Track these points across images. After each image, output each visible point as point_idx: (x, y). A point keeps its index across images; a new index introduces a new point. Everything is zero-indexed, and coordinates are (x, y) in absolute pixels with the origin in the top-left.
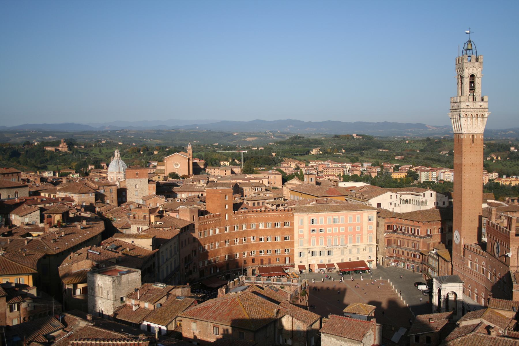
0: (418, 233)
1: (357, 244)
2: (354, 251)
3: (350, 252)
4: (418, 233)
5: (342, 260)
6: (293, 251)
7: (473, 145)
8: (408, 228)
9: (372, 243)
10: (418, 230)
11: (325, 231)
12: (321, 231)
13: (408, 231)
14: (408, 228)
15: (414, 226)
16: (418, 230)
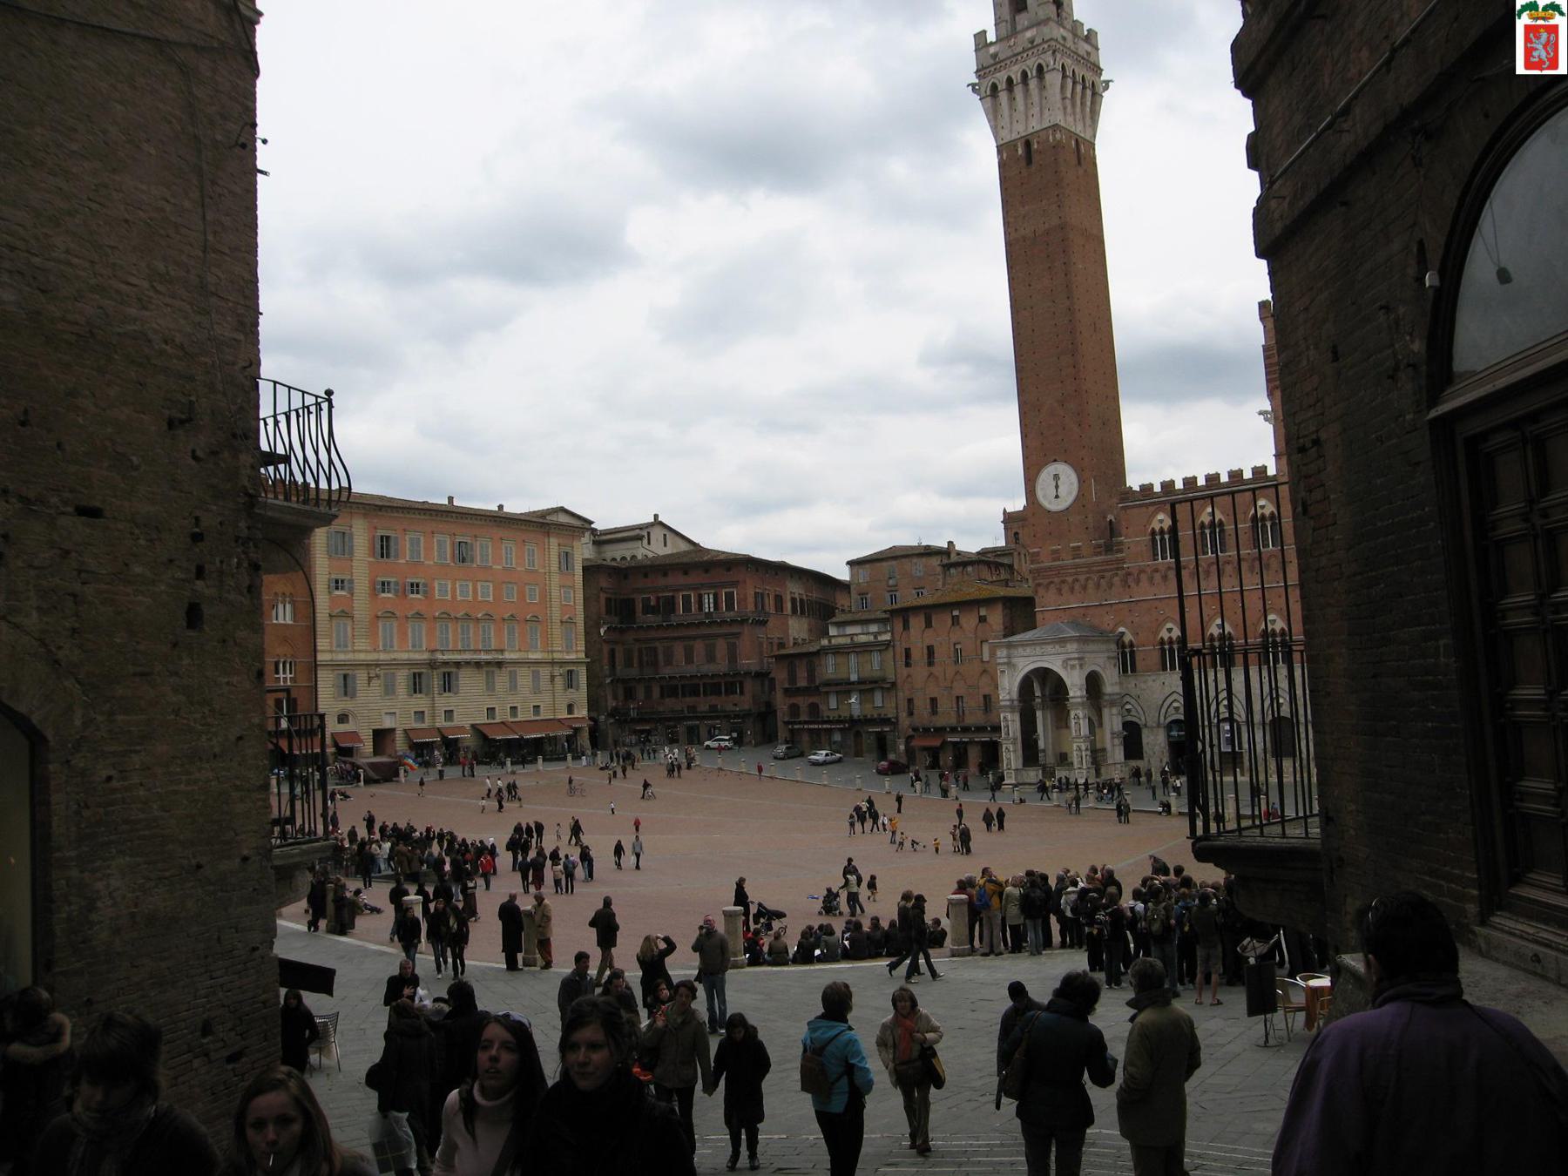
0: (730, 606)
1: (533, 656)
2: (524, 678)
3: (513, 686)
4: (730, 606)
5: (491, 711)
6: (314, 667)
7: (1081, 171)
8: (687, 599)
9: (573, 656)
10: (730, 597)
11: (428, 595)
12: (415, 587)
13: (687, 608)
14: (687, 599)
15: (711, 586)
16: (730, 597)
